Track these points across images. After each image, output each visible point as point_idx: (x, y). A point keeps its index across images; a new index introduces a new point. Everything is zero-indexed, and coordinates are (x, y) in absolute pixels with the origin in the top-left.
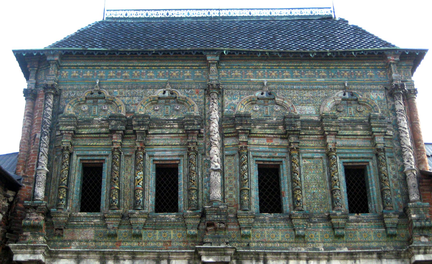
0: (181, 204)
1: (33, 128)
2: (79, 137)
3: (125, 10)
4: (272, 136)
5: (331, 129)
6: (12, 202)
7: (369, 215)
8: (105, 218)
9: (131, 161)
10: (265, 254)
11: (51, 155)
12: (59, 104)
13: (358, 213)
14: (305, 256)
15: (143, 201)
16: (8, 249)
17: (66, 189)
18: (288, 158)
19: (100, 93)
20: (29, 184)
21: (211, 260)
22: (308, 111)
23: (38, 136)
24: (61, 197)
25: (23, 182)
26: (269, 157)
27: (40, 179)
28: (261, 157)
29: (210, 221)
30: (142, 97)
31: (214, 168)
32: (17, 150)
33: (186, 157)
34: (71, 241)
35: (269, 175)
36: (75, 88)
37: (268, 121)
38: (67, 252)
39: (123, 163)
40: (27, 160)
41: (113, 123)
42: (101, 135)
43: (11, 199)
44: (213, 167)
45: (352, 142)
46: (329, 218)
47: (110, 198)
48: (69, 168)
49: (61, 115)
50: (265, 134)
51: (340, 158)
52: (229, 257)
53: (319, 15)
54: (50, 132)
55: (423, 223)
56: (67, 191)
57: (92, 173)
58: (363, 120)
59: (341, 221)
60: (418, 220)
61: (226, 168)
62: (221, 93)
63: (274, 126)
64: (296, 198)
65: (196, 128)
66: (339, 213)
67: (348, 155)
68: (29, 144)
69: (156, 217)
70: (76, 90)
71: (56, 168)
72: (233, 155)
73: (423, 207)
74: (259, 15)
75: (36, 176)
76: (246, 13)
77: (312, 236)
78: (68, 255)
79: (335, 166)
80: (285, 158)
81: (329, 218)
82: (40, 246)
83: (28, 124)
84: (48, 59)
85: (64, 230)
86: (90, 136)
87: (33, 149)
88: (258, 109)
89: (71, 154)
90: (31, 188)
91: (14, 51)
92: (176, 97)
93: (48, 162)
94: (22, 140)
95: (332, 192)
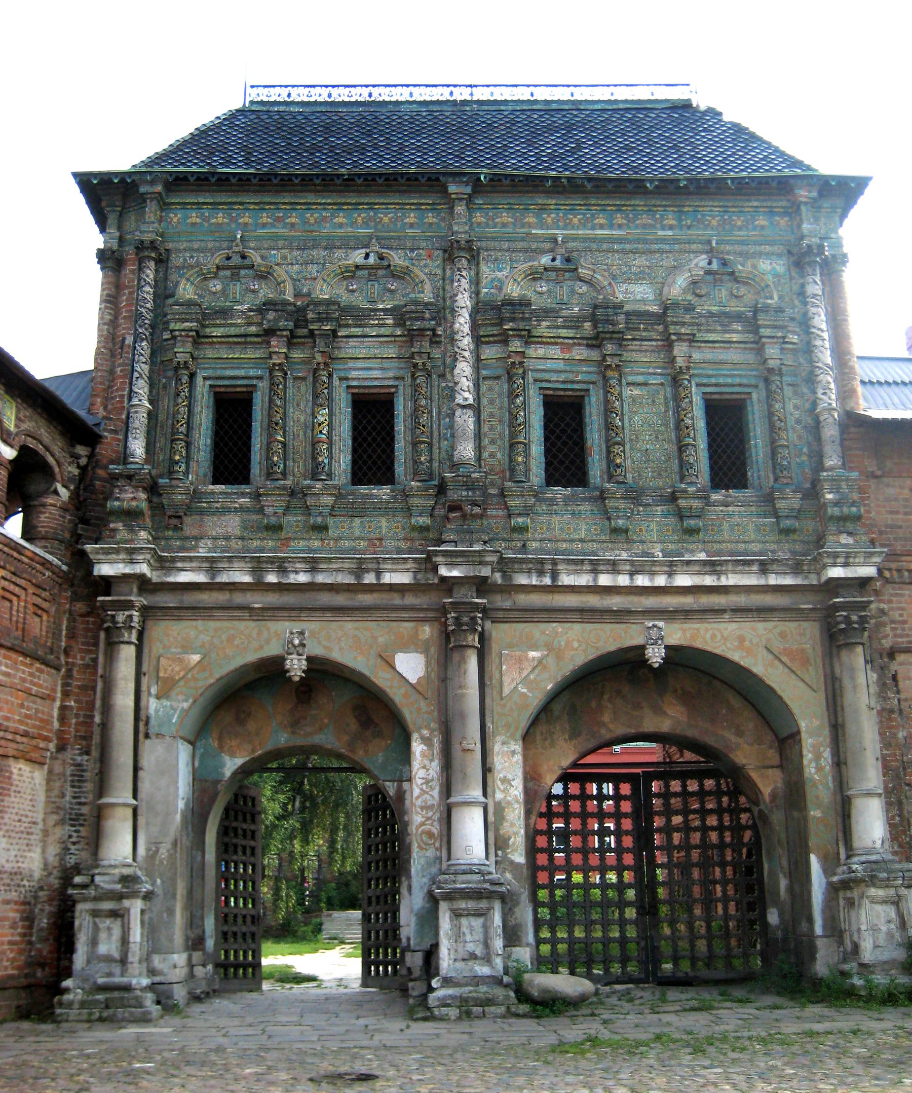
0: (400, 469)
1: (118, 326)
2: (206, 343)
3: (286, 86)
4: (571, 341)
5: (683, 331)
6: (86, 466)
7: (748, 492)
8: (260, 495)
9: (305, 389)
10: (555, 563)
11: (155, 377)
12: (166, 279)
13: (727, 489)
14: (628, 568)
15: (330, 464)
16: (83, 553)
17: (186, 442)
18: (600, 383)
19: (244, 257)
20: (115, 432)
21: (455, 573)
22: (639, 294)
23: (129, 340)
24: (177, 458)
25: (105, 430)
26: (564, 382)
27: (137, 424)
28: (549, 381)
29: (453, 501)
30: (324, 265)
31: (461, 402)
32: (90, 366)
33: (408, 380)
34: (198, 538)
35: (564, 416)
36: (196, 246)
37: (565, 313)
38: (191, 559)
39: (290, 392)
40: (110, 387)
41: (271, 315)
42: (249, 339)
43: (83, 461)
44: (459, 400)
45: (721, 355)
46: (673, 498)
47: (268, 458)
48: (190, 403)
49: (170, 301)
50: (559, 337)
51: (698, 385)
52: (489, 568)
53: (667, 101)
54: (151, 334)
55: (846, 510)
56: (188, 445)
57: (233, 410)
58: (743, 313)
59: (696, 504)
60: (836, 504)
61: (485, 401)
62: (474, 258)
63: (574, 323)
64: (613, 461)
65: (428, 326)
66: (691, 489)
67: (713, 380)
68: (113, 355)
69: (353, 494)
70: (197, 250)
71: (165, 402)
72: (497, 378)
73: (847, 480)
74: (549, 98)
75: (128, 418)
76: (523, 94)
77: (641, 530)
78: (194, 564)
79: (687, 400)
80: (593, 383)
81: (673, 498)
82: (142, 548)
83: (108, 317)
84: (142, 190)
85: (185, 518)
86: (228, 341)
87: (119, 365)
88: (544, 289)
89: (192, 376)
90: (119, 440)
91: (75, 175)
92: (389, 266)
93: (150, 392)
94: (98, 348)
95: (681, 448)
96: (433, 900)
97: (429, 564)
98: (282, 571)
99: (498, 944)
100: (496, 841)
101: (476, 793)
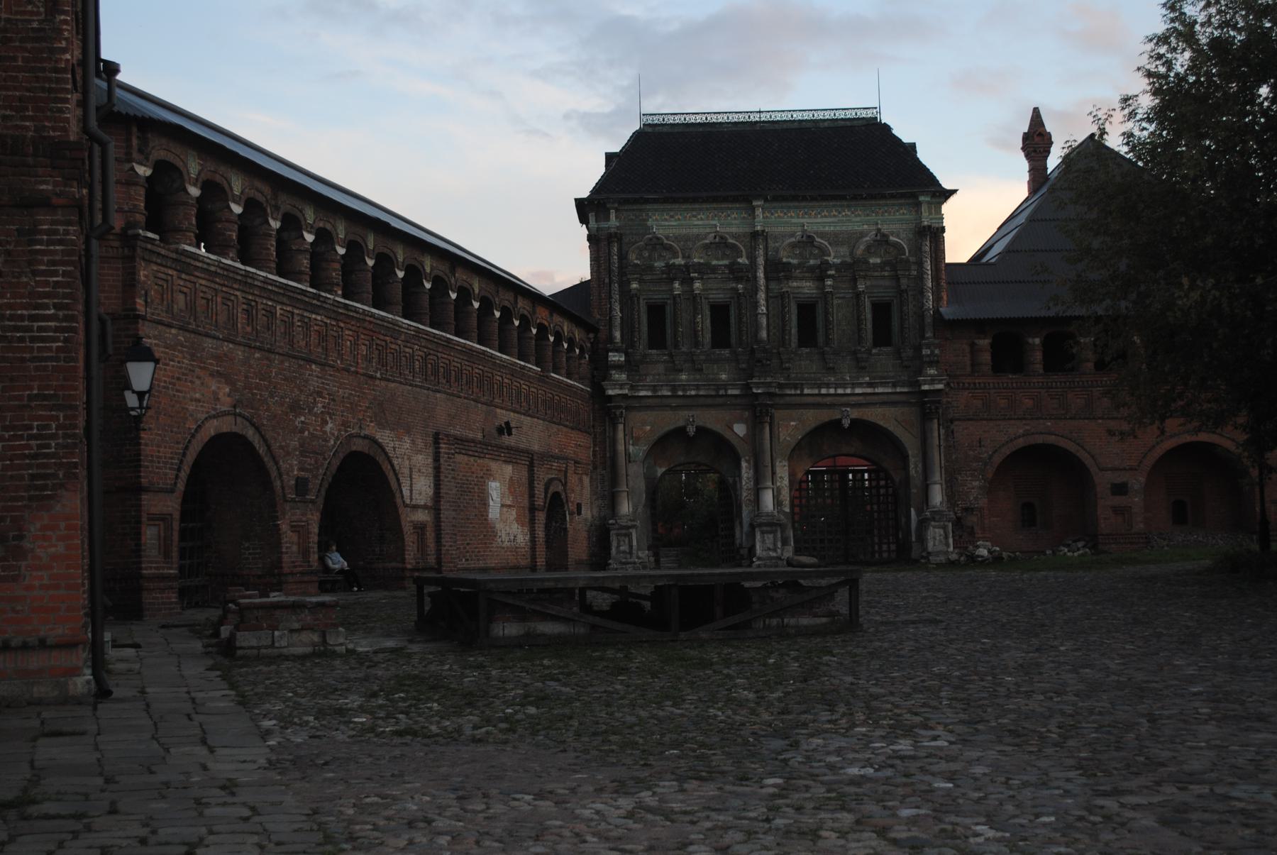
7: (889, 349)
23: (607, 281)
46: (855, 353)
57: (656, 311)
96: (752, 527)
97: (748, 387)
98: (684, 390)
99: (779, 545)
100: (778, 502)
101: (769, 484)
